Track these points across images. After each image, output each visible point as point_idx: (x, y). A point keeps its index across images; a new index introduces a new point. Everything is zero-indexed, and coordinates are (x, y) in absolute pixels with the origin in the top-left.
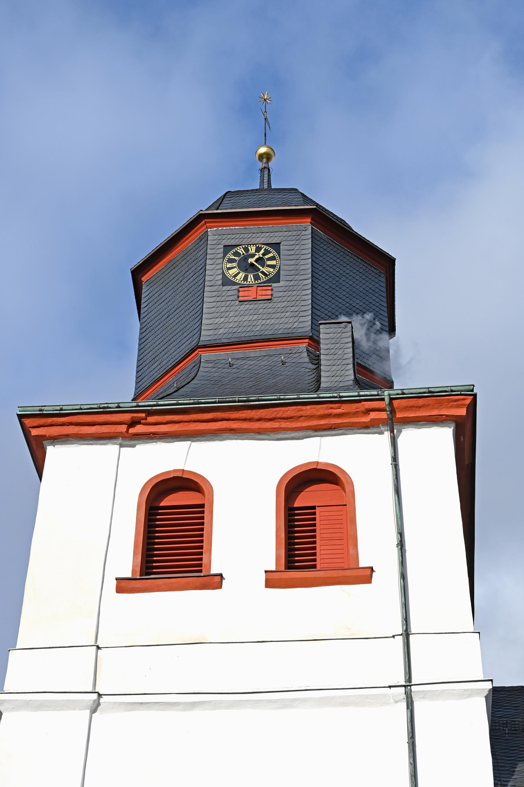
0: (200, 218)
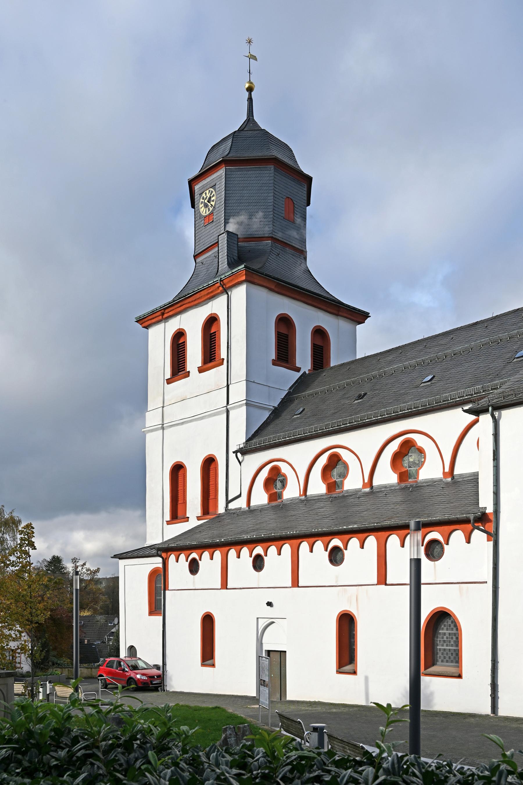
0: (192, 183)
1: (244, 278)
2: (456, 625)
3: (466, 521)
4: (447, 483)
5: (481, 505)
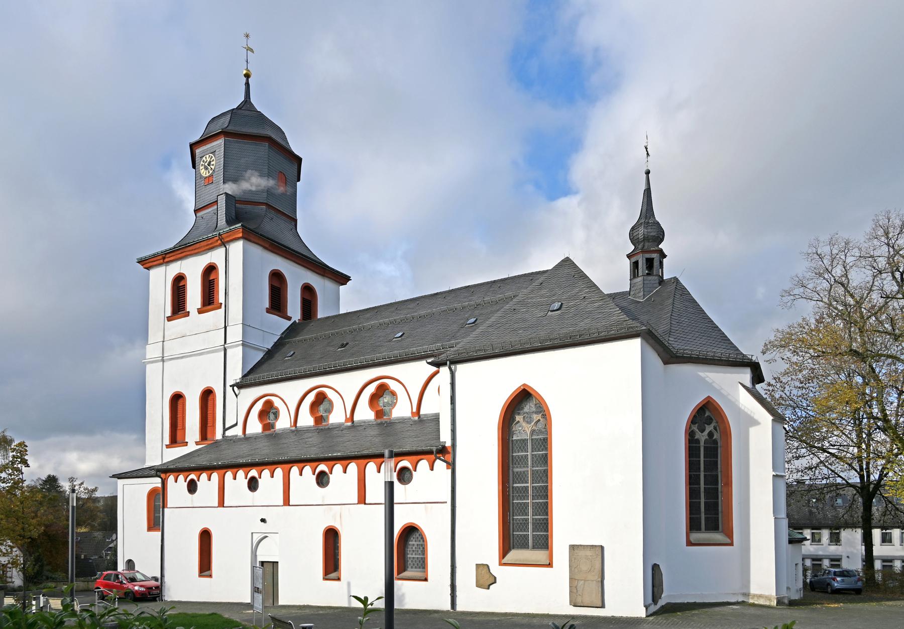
1: (241, 235)
2: (423, 538)
3: (430, 452)
4: (415, 421)
5: (442, 440)
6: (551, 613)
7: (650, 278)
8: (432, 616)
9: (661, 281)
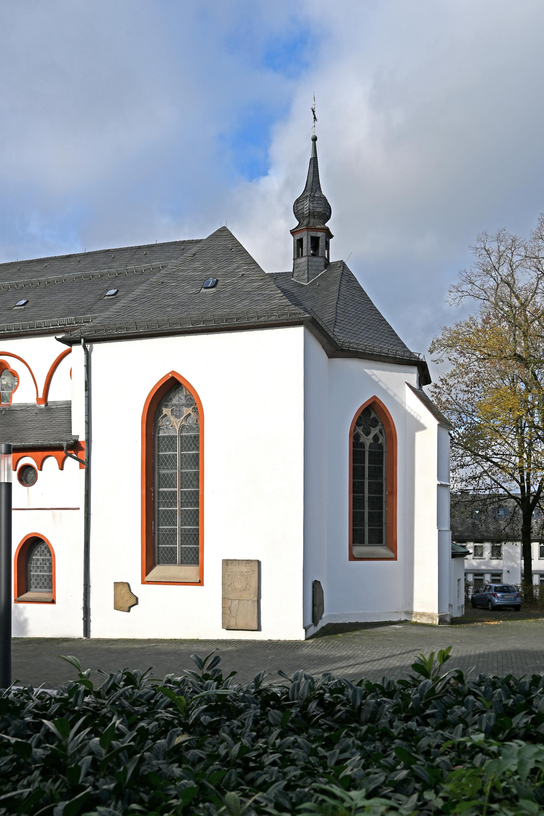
2: (50, 551)
3: (59, 448)
4: (41, 409)
5: (74, 433)
6: (201, 638)
7: (315, 259)
8: (61, 645)
9: (327, 264)
